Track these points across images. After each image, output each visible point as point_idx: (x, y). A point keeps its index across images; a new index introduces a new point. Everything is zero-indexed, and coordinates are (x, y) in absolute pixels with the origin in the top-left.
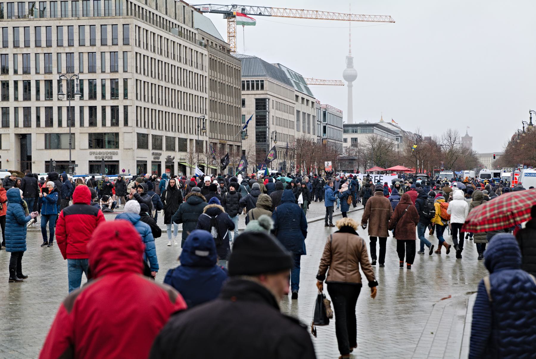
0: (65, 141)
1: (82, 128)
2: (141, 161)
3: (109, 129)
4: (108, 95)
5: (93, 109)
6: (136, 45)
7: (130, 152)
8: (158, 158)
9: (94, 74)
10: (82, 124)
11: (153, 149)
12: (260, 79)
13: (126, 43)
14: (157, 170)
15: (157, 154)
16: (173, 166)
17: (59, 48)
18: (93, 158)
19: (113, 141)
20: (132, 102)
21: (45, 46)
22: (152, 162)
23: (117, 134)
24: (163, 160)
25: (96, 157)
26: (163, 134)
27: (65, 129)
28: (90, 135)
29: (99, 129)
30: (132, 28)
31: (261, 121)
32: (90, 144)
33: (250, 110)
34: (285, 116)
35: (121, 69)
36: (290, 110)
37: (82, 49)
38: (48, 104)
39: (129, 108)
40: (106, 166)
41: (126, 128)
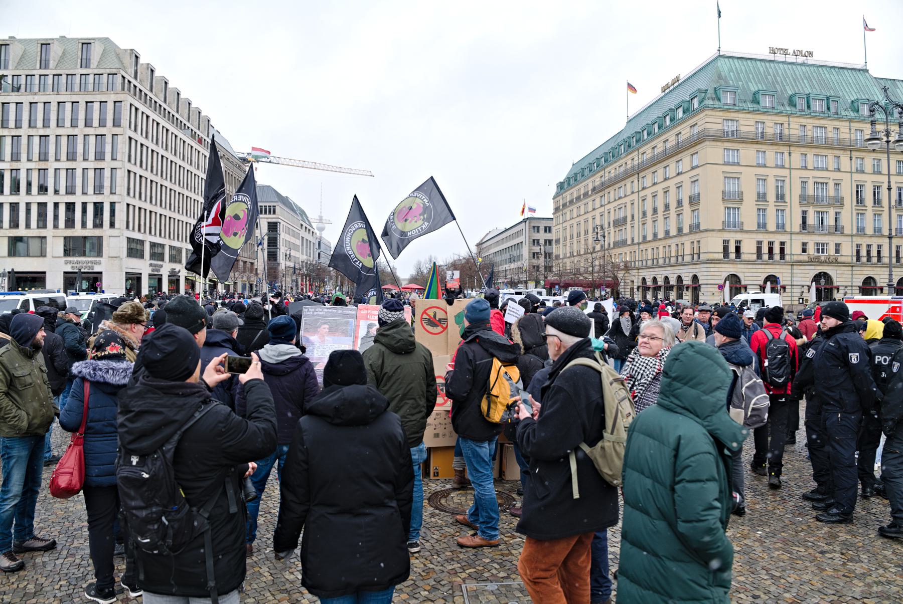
0: (34, 246)
1: (56, 230)
2: (133, 273)
3: (90, 231)
4: (90, 190)
5: (70, 207)
7: (117, 261)
8: (158, 271)
9: (74, 163)
10: (56, 226)
12: (272, 204)
13: (116, 123)
14: (156, 285)
15: (156, 265)
16: (178, 280)
17: (30, 130)
18: (69, 269)
19: (96, 246)
20: (122, 199)
21: (13, 126)
22: (150, 275)
23: (100, 238)
24: (165, 272)
25: (73, 267)
26: (166, 242)
27: (34, 231)
28: (65, 238)
29: (78, 231)
31: (273, 242)
32: (65, 250)
34: (293, 240)
35: (108, 156)
36: (296, 236)
37: (60, 131)
38: (14, 199)
39: (117, 205)
40: (83, 279)
41: (112, 230)
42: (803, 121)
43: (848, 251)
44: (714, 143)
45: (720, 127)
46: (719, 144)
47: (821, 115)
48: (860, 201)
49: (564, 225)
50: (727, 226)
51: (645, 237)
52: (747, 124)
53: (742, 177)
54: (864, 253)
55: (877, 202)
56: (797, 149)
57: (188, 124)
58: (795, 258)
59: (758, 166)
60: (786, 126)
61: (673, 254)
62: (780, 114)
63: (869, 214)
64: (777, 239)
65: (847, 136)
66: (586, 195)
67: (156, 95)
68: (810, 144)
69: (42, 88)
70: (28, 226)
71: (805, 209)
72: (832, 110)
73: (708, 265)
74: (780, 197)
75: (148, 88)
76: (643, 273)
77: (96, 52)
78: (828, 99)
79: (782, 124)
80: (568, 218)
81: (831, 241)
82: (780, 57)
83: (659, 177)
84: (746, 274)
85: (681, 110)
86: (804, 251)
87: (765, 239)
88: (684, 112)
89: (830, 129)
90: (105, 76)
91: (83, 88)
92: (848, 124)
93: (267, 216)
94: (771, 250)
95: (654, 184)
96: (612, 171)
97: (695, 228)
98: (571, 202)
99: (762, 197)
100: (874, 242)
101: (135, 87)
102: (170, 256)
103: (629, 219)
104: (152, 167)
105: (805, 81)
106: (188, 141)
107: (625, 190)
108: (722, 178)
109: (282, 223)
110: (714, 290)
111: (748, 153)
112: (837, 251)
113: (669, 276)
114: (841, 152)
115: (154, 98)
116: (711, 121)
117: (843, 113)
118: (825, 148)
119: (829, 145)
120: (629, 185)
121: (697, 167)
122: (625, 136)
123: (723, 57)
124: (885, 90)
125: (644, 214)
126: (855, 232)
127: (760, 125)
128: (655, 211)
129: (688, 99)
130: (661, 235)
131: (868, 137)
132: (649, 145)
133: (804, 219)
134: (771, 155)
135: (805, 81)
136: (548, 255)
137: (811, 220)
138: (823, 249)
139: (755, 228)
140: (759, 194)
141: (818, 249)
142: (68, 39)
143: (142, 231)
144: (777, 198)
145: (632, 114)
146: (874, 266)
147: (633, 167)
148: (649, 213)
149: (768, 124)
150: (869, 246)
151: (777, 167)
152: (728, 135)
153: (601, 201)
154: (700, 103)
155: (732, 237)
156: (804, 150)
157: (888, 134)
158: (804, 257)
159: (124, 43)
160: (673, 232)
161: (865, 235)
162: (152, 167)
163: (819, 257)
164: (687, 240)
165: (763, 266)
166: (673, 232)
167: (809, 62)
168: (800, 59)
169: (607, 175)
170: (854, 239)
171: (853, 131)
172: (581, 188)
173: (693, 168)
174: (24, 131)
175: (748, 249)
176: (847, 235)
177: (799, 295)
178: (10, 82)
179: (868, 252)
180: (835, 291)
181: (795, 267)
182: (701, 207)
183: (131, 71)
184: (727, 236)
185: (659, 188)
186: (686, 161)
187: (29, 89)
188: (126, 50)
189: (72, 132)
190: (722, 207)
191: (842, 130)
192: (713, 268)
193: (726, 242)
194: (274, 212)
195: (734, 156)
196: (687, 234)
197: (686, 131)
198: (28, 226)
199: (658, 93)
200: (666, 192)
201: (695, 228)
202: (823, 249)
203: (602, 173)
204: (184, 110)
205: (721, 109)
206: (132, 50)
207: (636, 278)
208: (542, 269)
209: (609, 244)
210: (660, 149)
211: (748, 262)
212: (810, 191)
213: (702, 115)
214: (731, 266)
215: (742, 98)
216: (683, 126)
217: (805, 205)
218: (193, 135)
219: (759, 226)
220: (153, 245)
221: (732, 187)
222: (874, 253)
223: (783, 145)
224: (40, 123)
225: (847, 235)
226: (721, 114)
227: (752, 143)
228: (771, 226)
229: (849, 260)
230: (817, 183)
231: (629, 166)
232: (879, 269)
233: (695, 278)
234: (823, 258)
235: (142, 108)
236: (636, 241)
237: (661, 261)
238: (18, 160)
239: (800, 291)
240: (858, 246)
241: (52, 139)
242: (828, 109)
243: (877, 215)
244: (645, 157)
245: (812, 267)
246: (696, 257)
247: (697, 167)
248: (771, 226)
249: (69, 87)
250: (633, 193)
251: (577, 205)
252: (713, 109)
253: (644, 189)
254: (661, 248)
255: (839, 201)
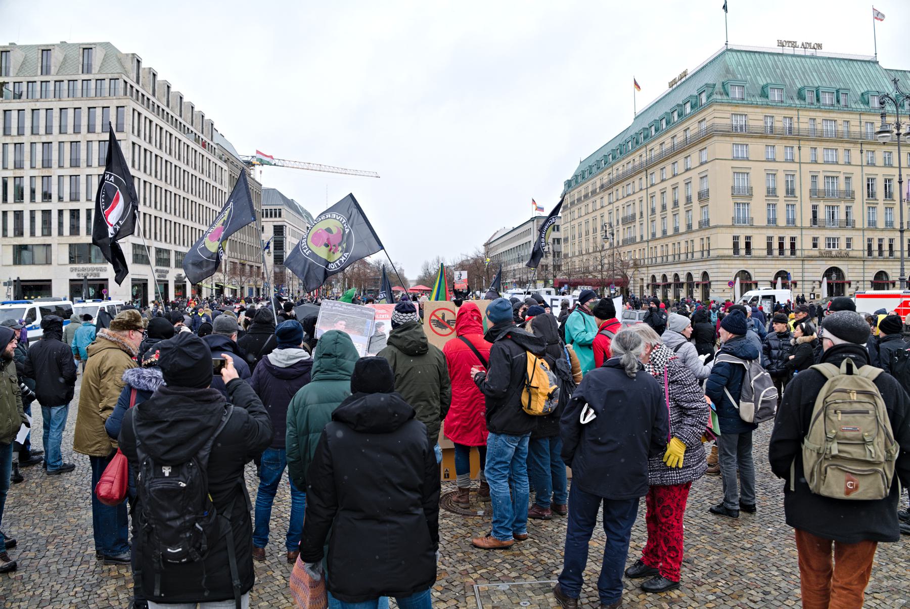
0: (39, 254)
1: (60, 238)
2: (139, 280)
6: (133, 132)
8: (165, 276)
9: (78, 169)
10: (60, 233)
11: (157, 264)
12: (278, 207)
15: (162, 271)
16: (184, 286)
17: (33, 137)
18: (74, 276)
24: (171, 278)
25: (78, 275)
27: (39, 239)
28: (71, 245)
30: (128, 112)
32: (70, 258)
33: (268, 235)
37: (63, 138)
38: (18, 207)
40: (90, 286)
42: (813, 114)
43: (859, 245)
44: (723, 138)
45: (728, 122)
46: (728, 139)
47: (831, 108)
48: (871, 195)
49: (572, 223)
50: (737, 222)
51: (654, 235)
52: (756, 118)
53: (751, 172)
54: (875, 247)
55: (888, 195)
56: (807, 143)
57: (191, 128)
58: (806, 253)
59: (768, 160)
60: (795, 119)
61: (683, 251)
62: (789, 107)
63: (881, 208)
64: (788, 235)
65: (857, 129)
66: (594, 192)
67: (158, 100)
68: (820, 138)
69: (44, 95)
70: (33, 234)
71: (815, 203)
72: (842, 103)
73: (718, 262)
74: (790, 192)
75: (151, 92)
76: (653, 271)
77: (97, 57)
78: (838, 91)
79: (791, 118)
80: (576, 217)
81: (842, 235)
82: (788, 50)
83: (668, 173)
84: (757, 270)
85: (688, 105)
86: (815, 246)
87: (776, 234)
88: (692, 107)
89: (840, 122)
90: (107, 81)
91: (85, 94)
92: (858, 117)
93: (273, 219)
94: (781, 245)
95: (663, 181)
96: (620, 168)
97: (705, 225)
98: (579, 200)
99: (771, 192)
100: (886, 236)
101: (137, 91)
102: (176, 261)
103: (638, 216)
104: (156, 172)
105: (814, 74)
106: (192, 145)
107: (634, 187)
108: (731, 174)
109: (288, 226)
110: (724, 287)
111: (757, 148)
112: (848, 246)
113: (679, 274)
114: (852, 145)
115: (157, 103)
116: (719, 116)
117: (853, 106)
118: (835, 141)
119: (838, 138)
120: (637, 182)
121: (706, 162)
122: (633, 133)
123: (731, 50)
124: (895, 81)
125: (653, 211)
126: (866, 226)
127: (769, 120)
128: (664, 207)
129: (696, 94)
130: (670, 232)
131: (878, 130)
132: (656, 142)
133: (815, 214)
134: (780, 149)
135: (814, 74)
136: (557, 254)
137: (822, 214)
138: (834, 244)
139: (765, 223)
140: (768, 188)
141: (829, 244)
142: (69, 45)
143: (148, 236)
144: (787, 192)
145: (639, 110)
146: (886, 260)
147: (641, 164)
148: (658, 209)
149: (777, 118)
150: (880, 240)
151: (786, 161)
152: (736, 130)
153: (609, 199)
154: (708, 98)
155: (742, 233)
156: (813, 144)
157: (898, 127)
158: (815, 252)
159: (125, 48)
160: (683, 229)
161: (876, 229)
162: (156, 172)
163: (831, 252)
164: (696, 237)
165: (773, 262)
166: (683, 229)
167: (818, 55)
168: (809, 52)
169: (614, 172)
170: (866, 233)
171: (863, 124)
172: (589, 186)
173: (702, 164)
174: (27, 139)
175: (759, 244)
176: (858, 229)
177: (810, 290)
178: (11, 88)
179: (880, 246)
180: (847, 286)
181: (806, 262)
182: (710, 203)
183: (134, 75)
184: (737, 232)
185: (668, 185)
186: (694, 157)
187: (30, 96)
188: (127, 55)
189: (75, 138)
190: (731, 202)
191: (852, 123)
192: (723, 264)
193: (736, 238)
194: (280, 216)
195: (742, 151)
196: (697, 231)
197: (693, 127)
198: (33, 234)
199: (666, 89)
200: (674, 189)
201: (705, 225)
202: (834, 244)
203: (610, 170)
204: (187, 113)
205: (729, 104)
206: (133, 54)
207: (645, 275)
208: (551, 268)
209: (618, 242)
210: (668, 145)
211: (759, 258)
212: (821, 185)
213: (710, 110)
214: (741, 262)
215: (751, 92)
216: (690, 122)
217: (816, 200)
218: (197, 139)
219: (769, 221)
220: (159, 251)
221: (741, 182)
222: (886, 247)
223: (793, 139)
224: (42, 130)
225: (858, 229)
226: (729, 108)
227: (761, 137)
228: (782, 222)
229: (860, 254)
230: (828, 177)
231: (637, 163)
232: (891, 263)
233: (705, 275)
234: (834, 253)
235: (145, 113)
236: (645, 238)
237: (670, 259)
238: (21, 168)
239: (811, 286)
240: (870, 240)
241: (55, 146)
242: (838, 101)
243: (889, 209)
244: (654, 153)
245: (824, 262)
246: (705, 253)
247: (706, 162)
248: (782, 222)
249: (71, 94)
250: (641, 190)
251: (586, 203)
252: (722, 103)
253: (652, 185)
254: (670, 245)
255: (849, 195)
